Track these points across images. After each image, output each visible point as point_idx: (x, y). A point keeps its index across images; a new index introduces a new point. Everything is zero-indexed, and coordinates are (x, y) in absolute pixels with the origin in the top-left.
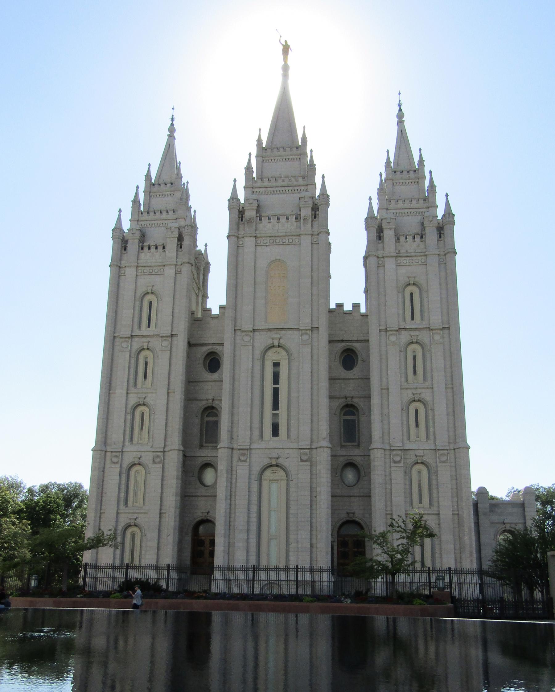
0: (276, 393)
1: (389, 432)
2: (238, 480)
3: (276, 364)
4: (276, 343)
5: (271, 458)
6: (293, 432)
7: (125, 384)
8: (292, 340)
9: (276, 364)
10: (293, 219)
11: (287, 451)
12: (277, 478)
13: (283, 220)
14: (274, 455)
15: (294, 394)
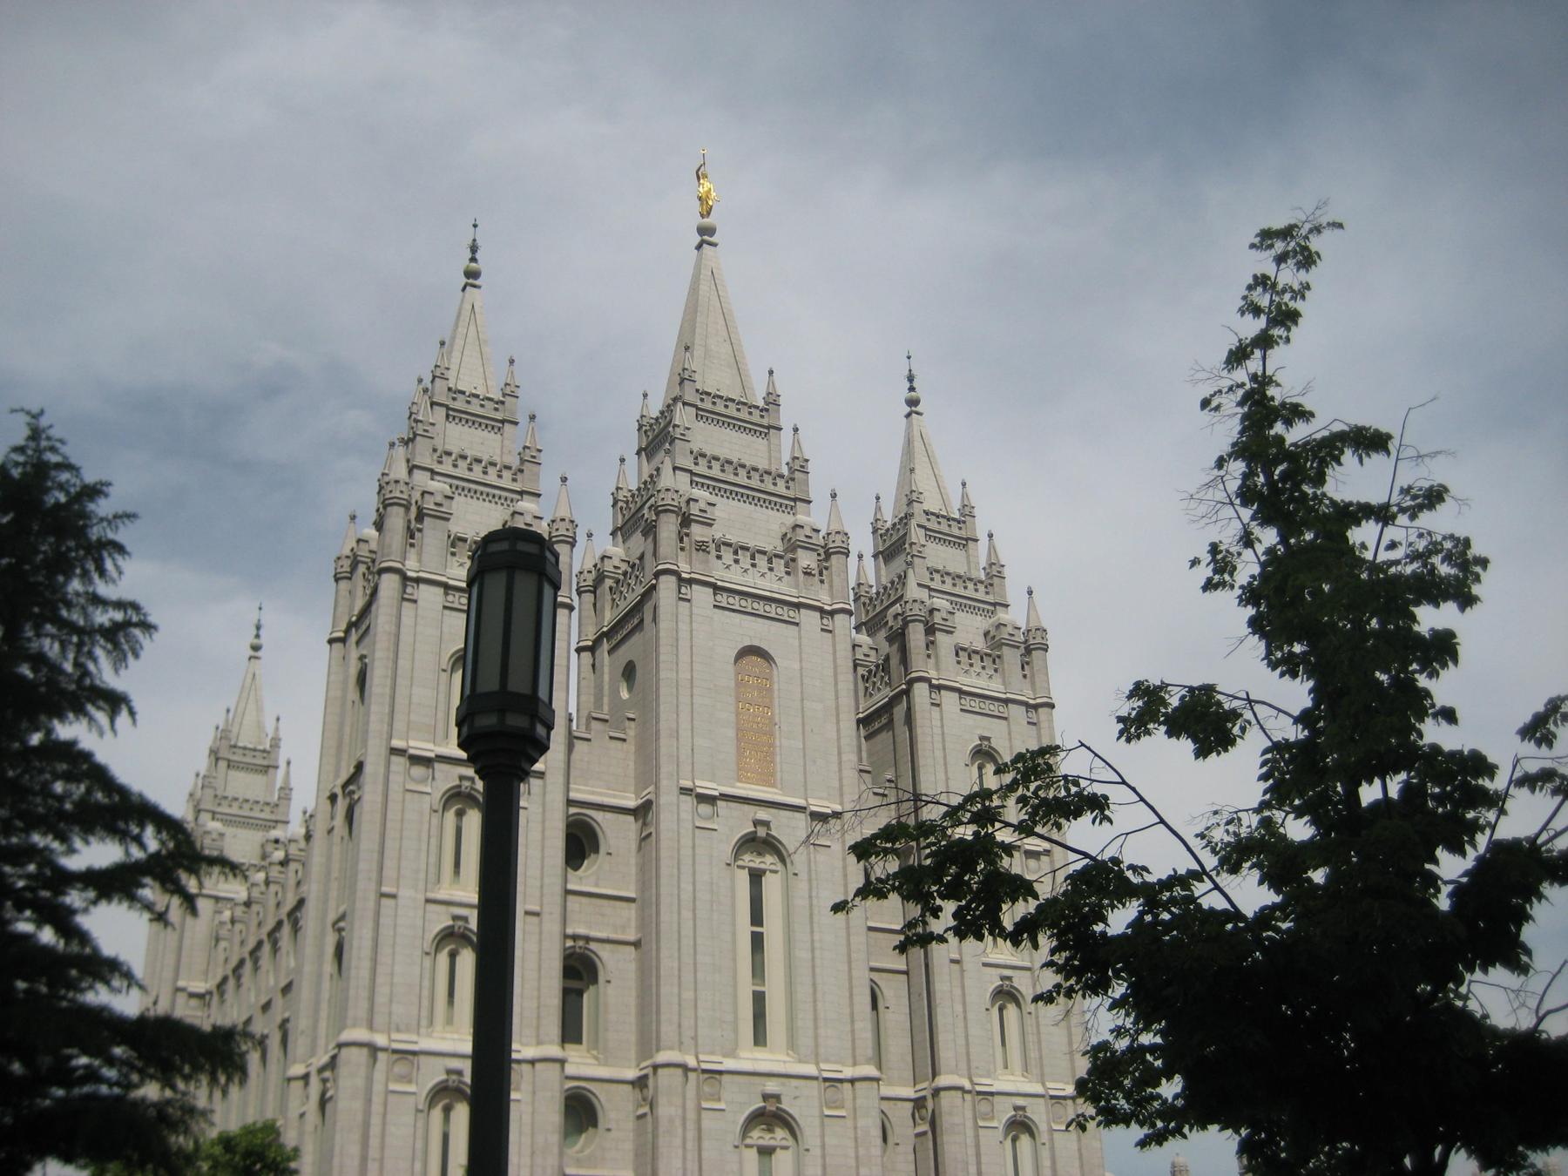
0: (757, 941)
1: (968, 1054)
2: (706, 1144)
3: (756, 877)
4: (762, 832)
5: (766, 1097)
6: (805, 1040)
7: (422, 875)
8: (790, 830)
9: (756, 877)
10: (779, 565)
11: (795, 1082)
12: (772, 1143)
13: (762, 562)
14: (772, 1086)
15: (802, 954)
